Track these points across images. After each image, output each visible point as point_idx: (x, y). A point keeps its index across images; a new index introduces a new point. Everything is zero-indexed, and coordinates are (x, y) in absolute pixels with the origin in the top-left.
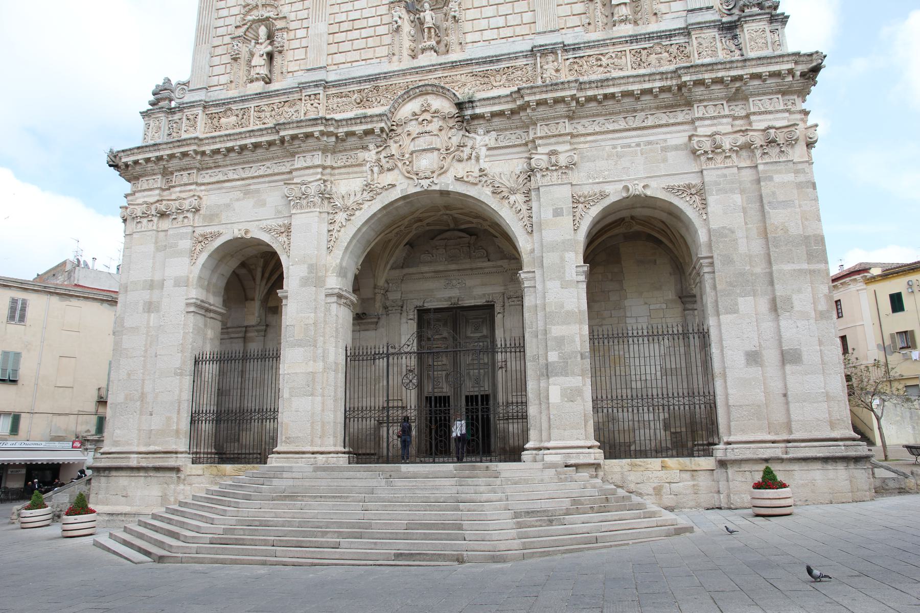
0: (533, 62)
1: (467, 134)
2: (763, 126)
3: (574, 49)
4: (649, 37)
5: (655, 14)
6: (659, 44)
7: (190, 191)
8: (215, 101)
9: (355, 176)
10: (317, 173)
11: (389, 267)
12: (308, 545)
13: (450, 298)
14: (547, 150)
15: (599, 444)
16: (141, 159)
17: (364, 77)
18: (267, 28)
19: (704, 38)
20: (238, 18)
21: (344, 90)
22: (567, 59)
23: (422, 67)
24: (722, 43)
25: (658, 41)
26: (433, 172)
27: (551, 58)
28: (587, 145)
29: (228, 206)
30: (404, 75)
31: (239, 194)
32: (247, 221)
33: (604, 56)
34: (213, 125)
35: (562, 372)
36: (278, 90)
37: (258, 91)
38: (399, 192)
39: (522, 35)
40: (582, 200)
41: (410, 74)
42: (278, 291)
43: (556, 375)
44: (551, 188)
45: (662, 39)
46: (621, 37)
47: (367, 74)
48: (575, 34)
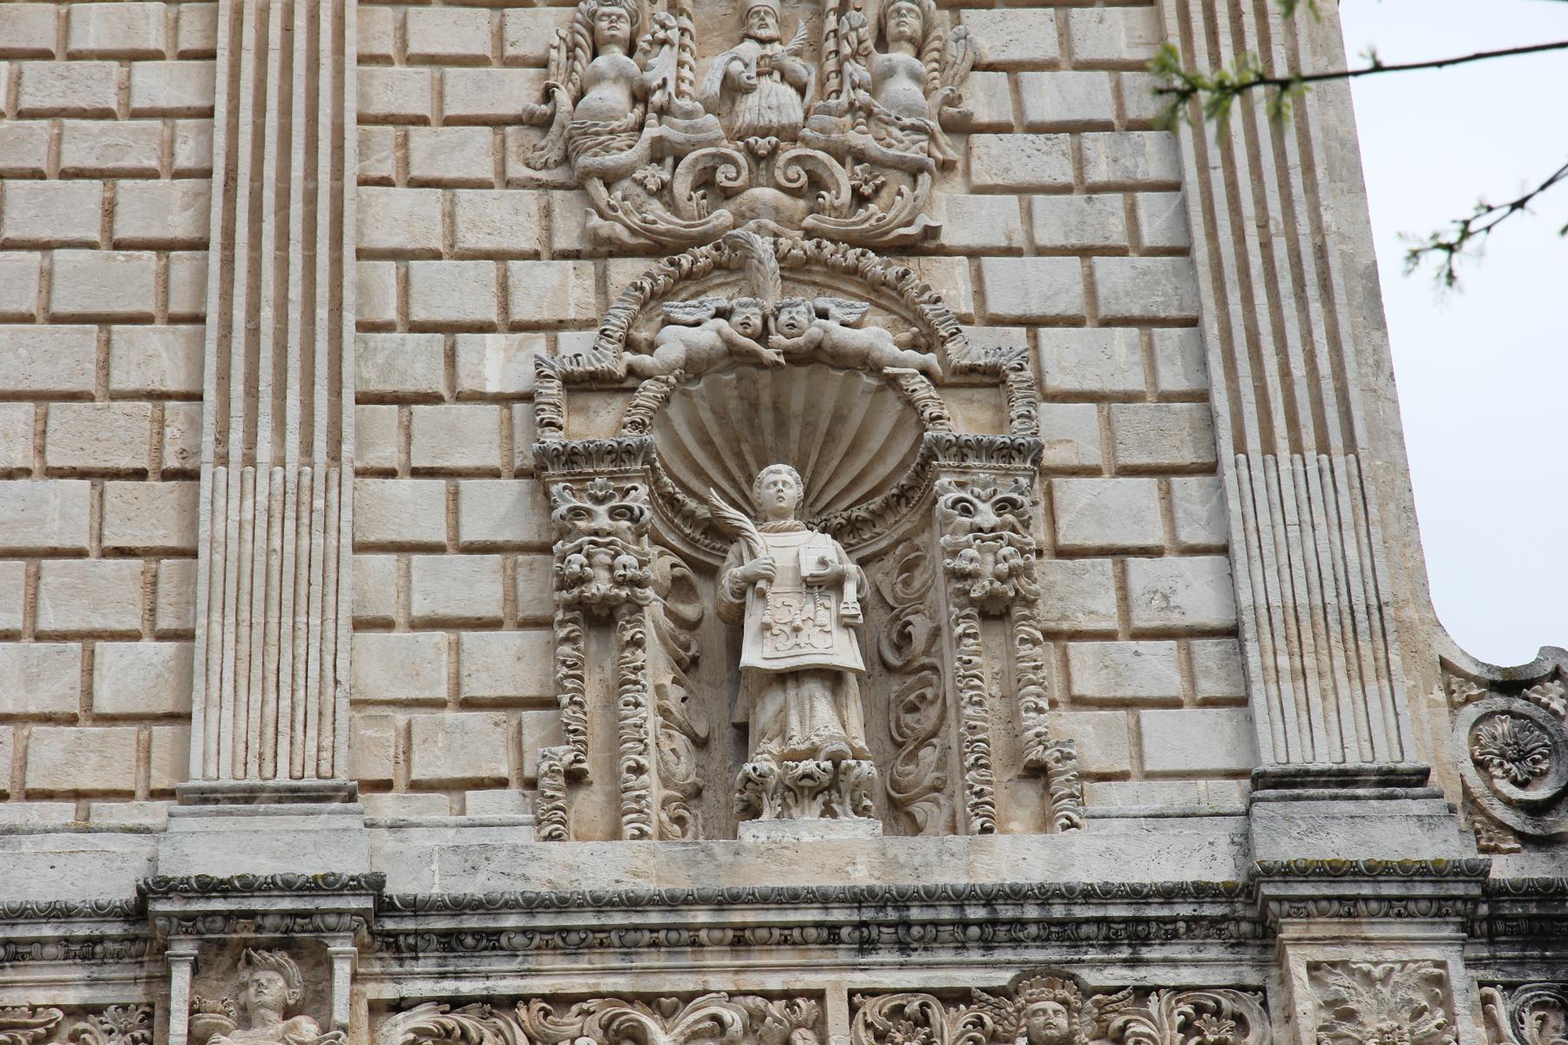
0: (136, 994)
3: (450, 941)
5: (1037, 772)
6: (1057, 975)
19: (1367, 977)
24: (1491, 1021)
25: (1052, 954)
33: (667, 1014)
39: (77, 795)
45: (1075, 943)
46: (793, 899)
48: (473, 837)
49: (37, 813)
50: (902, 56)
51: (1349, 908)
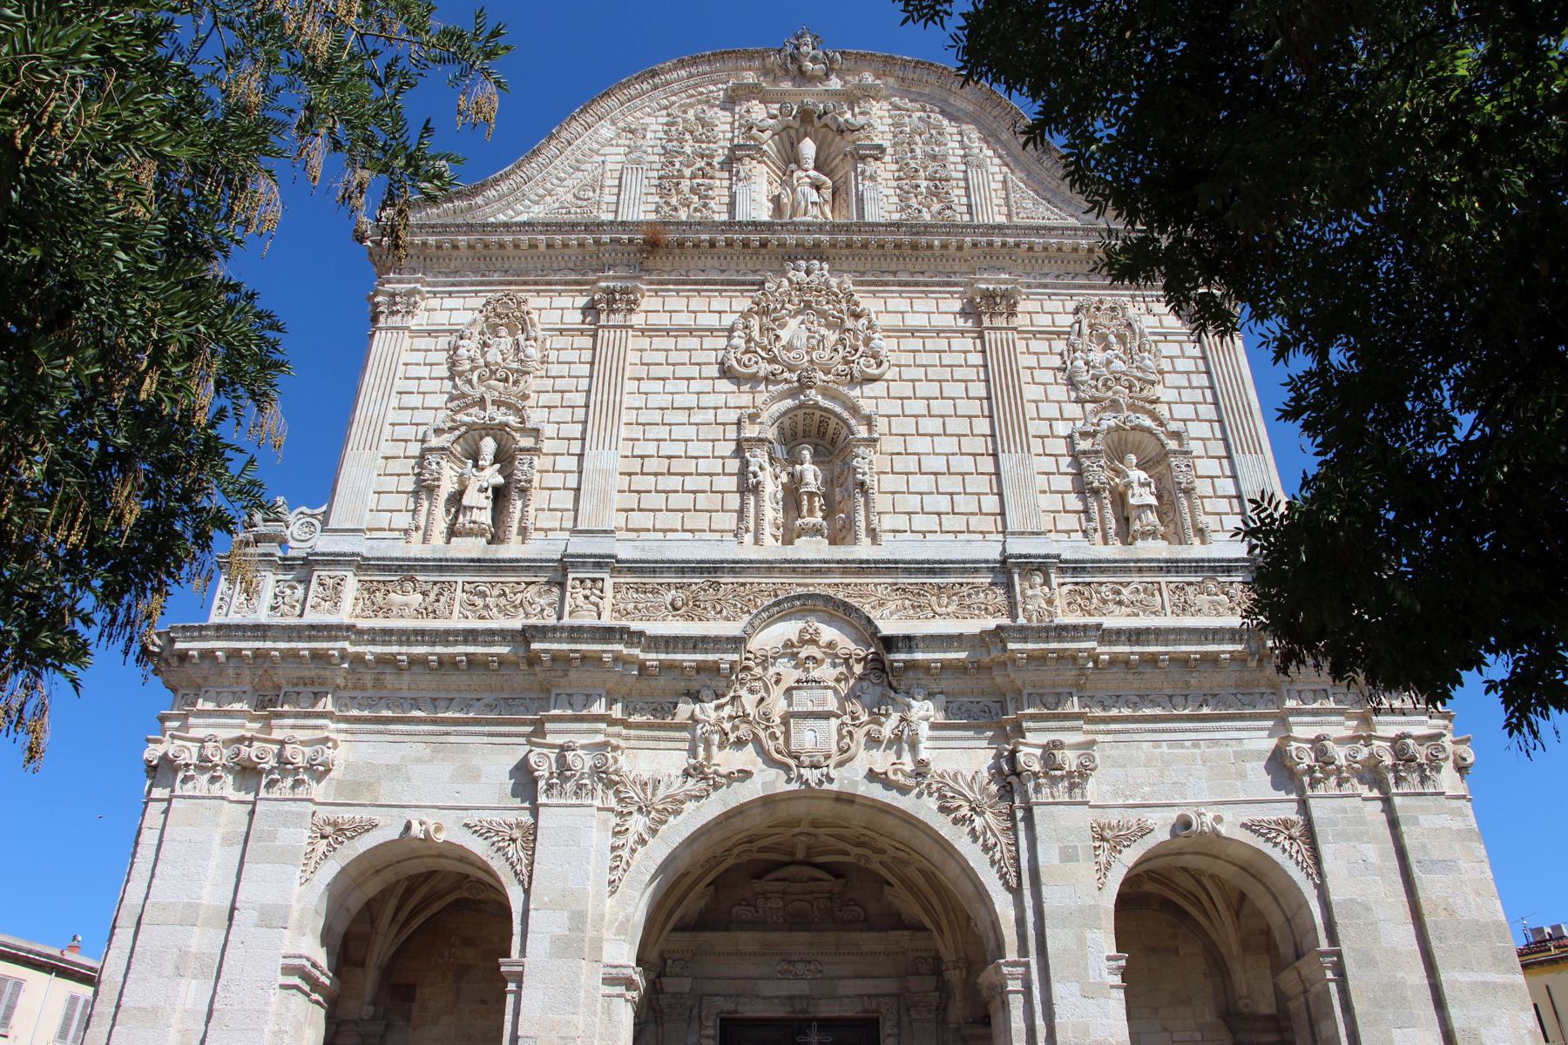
0: (1005, 580)
1: (892, 694)
2: (1392, 732)
4: (1197, 566)
5: (1201, 530)
6: (1213, 578)
7: (316, 727)
8: (384, 559)
9: (670, 745)
10: (597, 732)
11: (670, 926)
13: (792, 998)
14: (1044, 738)
16: (220, 649)
17: (692, 562)
20: (442, 414)
22: (1063, 584)
23: (804, 562)
26: (827, 757)
28: (1109, 738)
29: (395, 770)
31: (420, 749)
34: (373, 604)
36: (517, 560)
37: (475, 555)
38: (759, 786)
39: (981, 532)
40: (1108, 834)
41: (781, 570)
42: (501, 960)
44: (1052, 808)
45: (1216, 572)
46: (1152, 561)
47: (699, 558)
49: (972, 537)
50: (1146, 354)
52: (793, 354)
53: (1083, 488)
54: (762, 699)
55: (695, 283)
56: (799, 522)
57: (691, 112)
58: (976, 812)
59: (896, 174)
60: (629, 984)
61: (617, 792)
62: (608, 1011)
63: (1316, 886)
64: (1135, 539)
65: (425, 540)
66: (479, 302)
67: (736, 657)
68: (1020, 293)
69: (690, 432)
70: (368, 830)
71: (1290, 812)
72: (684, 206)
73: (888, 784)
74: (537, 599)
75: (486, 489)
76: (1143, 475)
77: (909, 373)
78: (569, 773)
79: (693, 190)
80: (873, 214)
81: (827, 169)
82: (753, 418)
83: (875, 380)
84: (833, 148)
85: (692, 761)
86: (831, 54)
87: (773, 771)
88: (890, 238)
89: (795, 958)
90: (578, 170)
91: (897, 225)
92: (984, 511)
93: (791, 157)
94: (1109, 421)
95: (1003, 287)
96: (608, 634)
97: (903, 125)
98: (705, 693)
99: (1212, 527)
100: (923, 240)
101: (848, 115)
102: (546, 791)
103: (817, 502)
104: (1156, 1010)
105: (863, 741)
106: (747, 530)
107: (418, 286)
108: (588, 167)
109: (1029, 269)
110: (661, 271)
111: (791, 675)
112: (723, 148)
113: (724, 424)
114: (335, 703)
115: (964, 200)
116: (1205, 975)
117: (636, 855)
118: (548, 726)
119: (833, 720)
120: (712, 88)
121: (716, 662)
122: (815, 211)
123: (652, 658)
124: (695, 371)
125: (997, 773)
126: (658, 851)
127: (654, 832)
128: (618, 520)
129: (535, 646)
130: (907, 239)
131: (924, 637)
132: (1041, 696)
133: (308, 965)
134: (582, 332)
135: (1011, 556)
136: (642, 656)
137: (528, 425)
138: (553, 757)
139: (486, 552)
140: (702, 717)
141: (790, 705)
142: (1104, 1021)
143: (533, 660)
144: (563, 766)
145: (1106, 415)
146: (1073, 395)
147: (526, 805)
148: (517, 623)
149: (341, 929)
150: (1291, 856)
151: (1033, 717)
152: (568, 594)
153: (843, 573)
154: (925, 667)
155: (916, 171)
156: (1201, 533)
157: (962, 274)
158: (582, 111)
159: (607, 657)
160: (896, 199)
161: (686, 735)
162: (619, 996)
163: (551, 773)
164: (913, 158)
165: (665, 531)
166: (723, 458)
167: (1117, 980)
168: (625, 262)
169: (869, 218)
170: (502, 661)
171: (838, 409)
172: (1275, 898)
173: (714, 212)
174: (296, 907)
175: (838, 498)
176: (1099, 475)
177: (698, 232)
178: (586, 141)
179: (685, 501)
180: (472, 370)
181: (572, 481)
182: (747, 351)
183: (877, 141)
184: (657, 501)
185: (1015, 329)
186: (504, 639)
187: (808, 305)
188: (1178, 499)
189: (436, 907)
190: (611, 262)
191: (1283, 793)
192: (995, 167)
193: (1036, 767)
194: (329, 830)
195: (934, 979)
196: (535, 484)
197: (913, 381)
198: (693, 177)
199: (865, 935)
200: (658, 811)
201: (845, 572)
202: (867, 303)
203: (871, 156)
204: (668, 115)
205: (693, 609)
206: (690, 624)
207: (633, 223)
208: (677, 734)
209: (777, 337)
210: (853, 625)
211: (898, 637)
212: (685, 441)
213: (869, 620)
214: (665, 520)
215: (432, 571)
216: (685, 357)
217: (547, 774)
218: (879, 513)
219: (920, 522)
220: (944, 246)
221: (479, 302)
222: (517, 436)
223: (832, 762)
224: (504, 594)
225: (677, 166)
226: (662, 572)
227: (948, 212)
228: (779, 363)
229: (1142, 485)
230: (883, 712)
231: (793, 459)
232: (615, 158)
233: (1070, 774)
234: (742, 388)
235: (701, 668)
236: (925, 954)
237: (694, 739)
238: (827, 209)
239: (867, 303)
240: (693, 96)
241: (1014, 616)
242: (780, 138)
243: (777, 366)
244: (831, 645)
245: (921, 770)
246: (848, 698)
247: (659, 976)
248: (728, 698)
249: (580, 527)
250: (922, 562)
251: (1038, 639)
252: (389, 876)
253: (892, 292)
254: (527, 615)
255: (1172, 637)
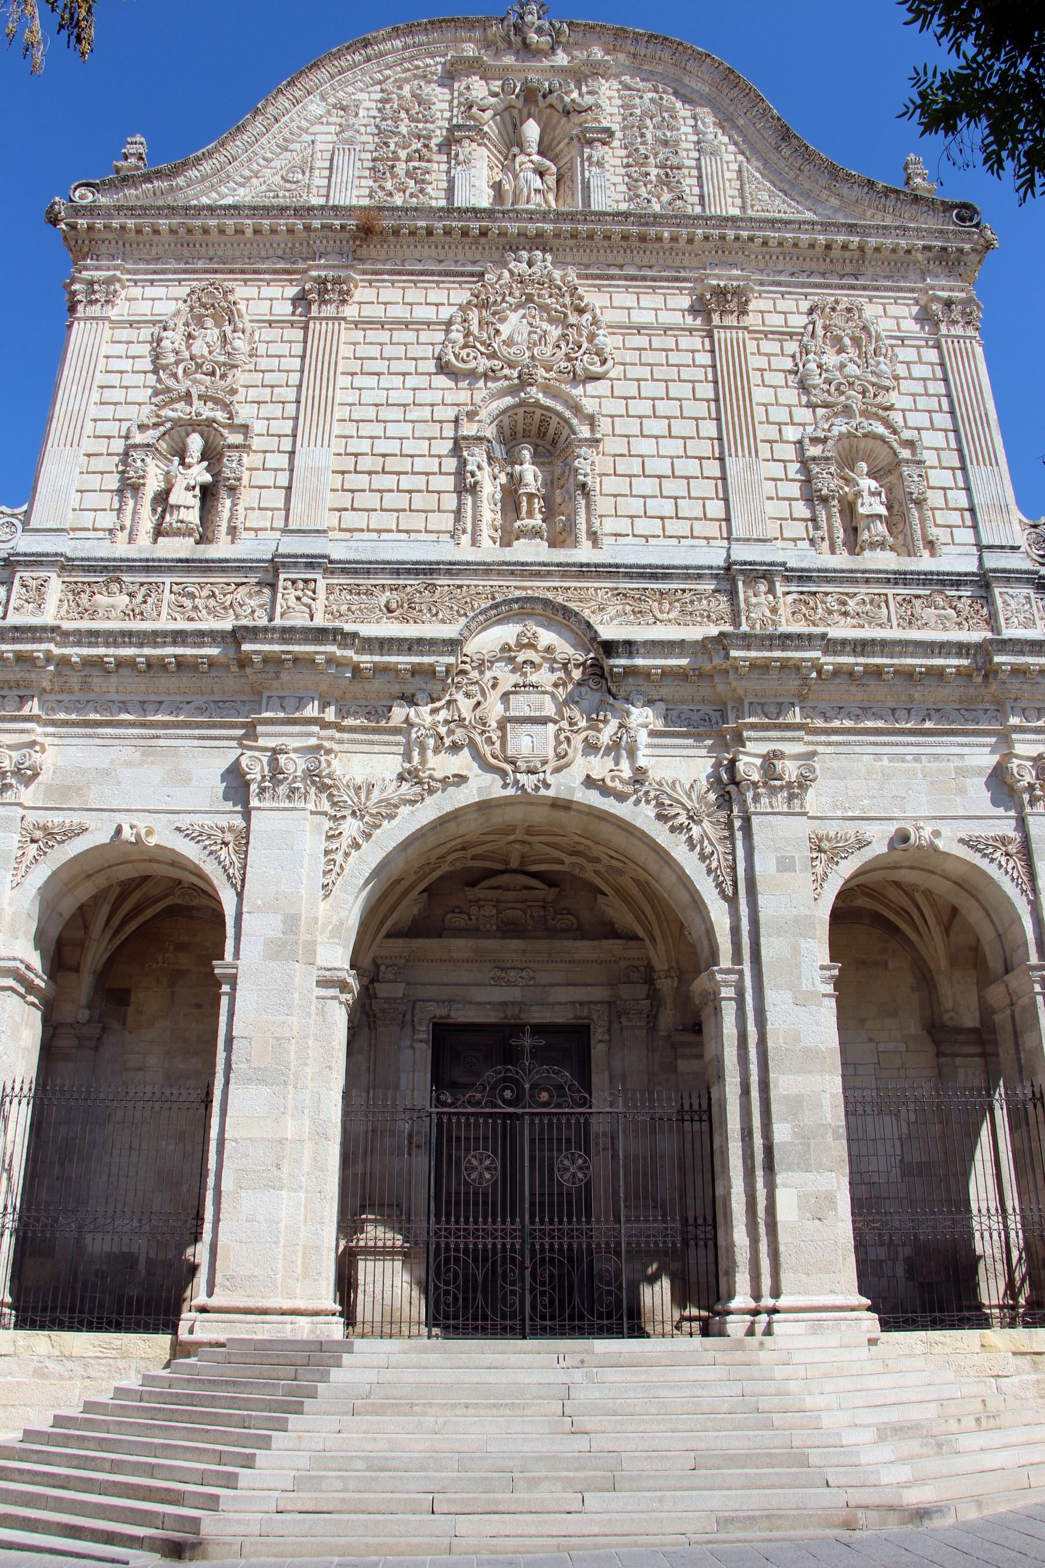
0: (728, 587)
1: (611, 700)
4: (925, 579)
5: (931, 542)
6: (941, 592)
7: (22, 731)
8: (88, 559)
9: (383, 749)
10: (309, 735)
11: (384, 931)
12: (512, 1508)
13: (504, 1004)
14: (764, 748)
15: (869, 1302)
17: (407, 563)
18: (202, 436)
20: (146, 410)
21: (365, 582)
23: (522, 564)
26: (544, 763)
27: (763, 587)
28: (830, 749)
29: (104, 774)
30: (487, 572)
31: (130, 753)
32: (149, 811)
34: (78, 605)
35: (799, 1164)
36: (227, 561)
37: (183, 555)
38: (475, 791)
39: (705, 538)
40: (826, 845)
41: (499, 573)
42: (215, 962)
43: (789, 1169)
47: (414, 558)
48: (801, 553)
49: (696, 542)
50: (882, 359)
51: (1008, 579)
52: (513, 350)
53: (812, 496)
54: (479, 704)
55: (412, 273)
56: (518, 523)
57: (407, 88)
58: (694, 821)
59: (625, 161)
60: (343, 987)
61: (331, 796)
62: (322, 1013)
63: (1030, 902)
64: (863, 549)
65: (131, 540)
66: (183, 291)
67: (451, 660)
68: (752, 291)
69: (406, 429)
70: (78, 834)
71: (1008, 828)
72: (399, 191)
73: (605, 791)
74: (248, 601)
75: (194, 488)
76: (874, 484)
77: (633, 372)
78: (281, 776)
79: (409, 174)
80: (600, 202)
81: (552, 155)
82: (471, 416)
83: (598, 379)
84: (558, 131)
85: (407, 765)
86: (557, 26)
87: (489, 777)
88: (617, 228)
89: (508, 965)
90: (286, 150)
91: (626, 215)
92: (709, 516)
93: (513, 141)
94: (841, 427)
95: (735, 284)
96: (320, 635)
97: (634, 106)
98: (420, 697)
99: (942, 540)
100: (652, 231)
101: (575, 95)
102: (258, 794)
103: (537, 504)
104: (862, 1021)
105: (581, 746)
106: (464, 532)
107: (118, 273)
108: (297, 146)
109: (762, 265)
110: (375, 261)
111: (508, 679)
112: (441, 128)
113: (441, 422)
114: (42, 705)
115: (696, 190)
116: (912, 989)
117: (350, 859)
118: (260, 729)
119: (550, 726)
120: (429, 61)
121: (431, 665)
122: (538, 199)
123: (366, 660)
124: (410, 366)
125: (716, 781)
126: (372, 855)
127: (368, 836)
128: (332, 520)
129: (246, 647)
130: (635, 229)
131: (645, 643)
132: (762, 705)
133: (22, 967)
134: (292, 324)
135: (736, 563)
136: (356, 658)
137: (237, 421)
138: (265, 760)
139: (194, 553)
140: (417, 721)
141: (507, 709)
142: (815, 1028)
143: (244, 662)
144: (276, 770)
145: (838, 421)
146: (804, 399)
147: (239, 808)
148: (227, 625)
149: (53, 933)
150: (1007, 872)
151: (753, 727)
152: (279, 595)
153: (563, 576)
154: (645, 674)
155: (646, 157)
156: (931, 545)
157: (692, 269)
158: (289, 83)
159: (320, 659)
160: (624, 188)
161: (400, 738)
162: (333, 998)
163: (264, 777)
164: (644, 143)
165: (379, 531)
166: (439, 456)
167: (829, 989)
168: (337, 250)
169: (595, 207)
170: (212, 663)
171: (560, 408)
172: (988, 915)
173: (431, 198)
174: (8, 910)
175: (559, 500)
176: (828, 482)
177: (414, 218)
178: (294, 119)
179: (401, 501)
180: (177, 363)
181: (283, 480)
182: (465, 346)
183: (605, 124)
184: (371, 500)
185: (746, 328)
186: (214, 640)
187: (530, 299)
188: (909, 509)
189: (149, 913)
190: (322, 249)
191: (1002, 809)
192: (730, 155)
193: (756, 777)
194: (38, 834)
195: (645, 987)
196: (245, 482)
197: (638, 380)
198: (409, 159)
199: (579, 943)
200: (371, 815)
201: (564, 575)
202: (592, 298)
203: (599, 140)
204: (382, 91)
205: (408, 611)
206: (405, 626)
207: (345, 208)
208: (391, 738)
209: (497, 331)
210: (572, 630)
211: (618, 642)
212: (401, 439)
213: (589, 625)
214: (378, 520)
215: (139, 571)
216: (400, 351)
217: (259, 778)
218: (601, 516)
219: (643, 526)
220: (674, 239)
221: (183, 291)
222: (225, 432)
223: (549, 768)
224: (214, 595)
225: (392, 147)
226: (376, 573)
227: (679, 203)
228: (498, 358)
229: (872, 494)
230: (601, 718)
231: (512, 459)
232: (325, 137)
233: (790, 785)
234: (460, 385)
235: (416, 671)
236: (636, 963)
237: (408, 742)
238: (551, 197)
239: (592, 298)
240: (409, 70)
241: (736, 623)
242: (502, 119)
243: (496, 362)
244: (549, 649)
245: (639, 777)
246: (566, 703)
247: (372, 981)
248: (443, 702)
249: (291, 527)
250: (644, 567)
251: (762, 647)
252: (101, 881)
253: (618, 286)
254: (237, 617)
255: (897, 649)
